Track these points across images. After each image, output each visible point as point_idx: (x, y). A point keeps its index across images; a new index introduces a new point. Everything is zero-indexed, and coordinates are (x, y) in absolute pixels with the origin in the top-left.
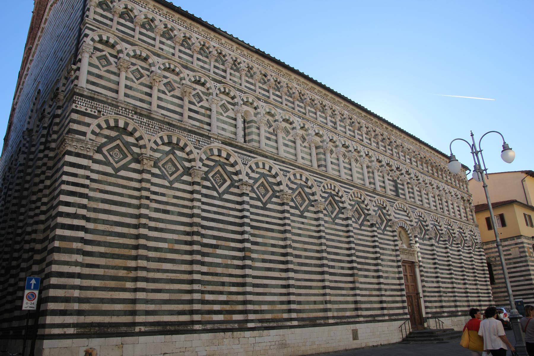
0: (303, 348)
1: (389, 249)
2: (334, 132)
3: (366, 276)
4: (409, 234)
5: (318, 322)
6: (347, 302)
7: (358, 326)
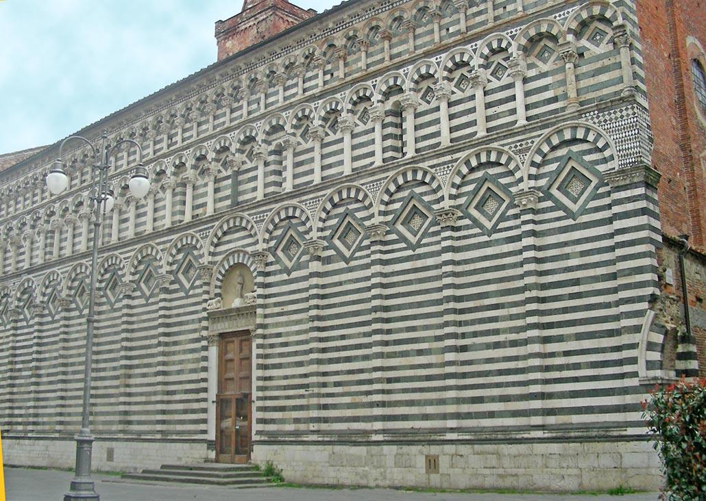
0: (60, 461)
1: (193, 321)
6: (114, 413)
7: (114, 444)
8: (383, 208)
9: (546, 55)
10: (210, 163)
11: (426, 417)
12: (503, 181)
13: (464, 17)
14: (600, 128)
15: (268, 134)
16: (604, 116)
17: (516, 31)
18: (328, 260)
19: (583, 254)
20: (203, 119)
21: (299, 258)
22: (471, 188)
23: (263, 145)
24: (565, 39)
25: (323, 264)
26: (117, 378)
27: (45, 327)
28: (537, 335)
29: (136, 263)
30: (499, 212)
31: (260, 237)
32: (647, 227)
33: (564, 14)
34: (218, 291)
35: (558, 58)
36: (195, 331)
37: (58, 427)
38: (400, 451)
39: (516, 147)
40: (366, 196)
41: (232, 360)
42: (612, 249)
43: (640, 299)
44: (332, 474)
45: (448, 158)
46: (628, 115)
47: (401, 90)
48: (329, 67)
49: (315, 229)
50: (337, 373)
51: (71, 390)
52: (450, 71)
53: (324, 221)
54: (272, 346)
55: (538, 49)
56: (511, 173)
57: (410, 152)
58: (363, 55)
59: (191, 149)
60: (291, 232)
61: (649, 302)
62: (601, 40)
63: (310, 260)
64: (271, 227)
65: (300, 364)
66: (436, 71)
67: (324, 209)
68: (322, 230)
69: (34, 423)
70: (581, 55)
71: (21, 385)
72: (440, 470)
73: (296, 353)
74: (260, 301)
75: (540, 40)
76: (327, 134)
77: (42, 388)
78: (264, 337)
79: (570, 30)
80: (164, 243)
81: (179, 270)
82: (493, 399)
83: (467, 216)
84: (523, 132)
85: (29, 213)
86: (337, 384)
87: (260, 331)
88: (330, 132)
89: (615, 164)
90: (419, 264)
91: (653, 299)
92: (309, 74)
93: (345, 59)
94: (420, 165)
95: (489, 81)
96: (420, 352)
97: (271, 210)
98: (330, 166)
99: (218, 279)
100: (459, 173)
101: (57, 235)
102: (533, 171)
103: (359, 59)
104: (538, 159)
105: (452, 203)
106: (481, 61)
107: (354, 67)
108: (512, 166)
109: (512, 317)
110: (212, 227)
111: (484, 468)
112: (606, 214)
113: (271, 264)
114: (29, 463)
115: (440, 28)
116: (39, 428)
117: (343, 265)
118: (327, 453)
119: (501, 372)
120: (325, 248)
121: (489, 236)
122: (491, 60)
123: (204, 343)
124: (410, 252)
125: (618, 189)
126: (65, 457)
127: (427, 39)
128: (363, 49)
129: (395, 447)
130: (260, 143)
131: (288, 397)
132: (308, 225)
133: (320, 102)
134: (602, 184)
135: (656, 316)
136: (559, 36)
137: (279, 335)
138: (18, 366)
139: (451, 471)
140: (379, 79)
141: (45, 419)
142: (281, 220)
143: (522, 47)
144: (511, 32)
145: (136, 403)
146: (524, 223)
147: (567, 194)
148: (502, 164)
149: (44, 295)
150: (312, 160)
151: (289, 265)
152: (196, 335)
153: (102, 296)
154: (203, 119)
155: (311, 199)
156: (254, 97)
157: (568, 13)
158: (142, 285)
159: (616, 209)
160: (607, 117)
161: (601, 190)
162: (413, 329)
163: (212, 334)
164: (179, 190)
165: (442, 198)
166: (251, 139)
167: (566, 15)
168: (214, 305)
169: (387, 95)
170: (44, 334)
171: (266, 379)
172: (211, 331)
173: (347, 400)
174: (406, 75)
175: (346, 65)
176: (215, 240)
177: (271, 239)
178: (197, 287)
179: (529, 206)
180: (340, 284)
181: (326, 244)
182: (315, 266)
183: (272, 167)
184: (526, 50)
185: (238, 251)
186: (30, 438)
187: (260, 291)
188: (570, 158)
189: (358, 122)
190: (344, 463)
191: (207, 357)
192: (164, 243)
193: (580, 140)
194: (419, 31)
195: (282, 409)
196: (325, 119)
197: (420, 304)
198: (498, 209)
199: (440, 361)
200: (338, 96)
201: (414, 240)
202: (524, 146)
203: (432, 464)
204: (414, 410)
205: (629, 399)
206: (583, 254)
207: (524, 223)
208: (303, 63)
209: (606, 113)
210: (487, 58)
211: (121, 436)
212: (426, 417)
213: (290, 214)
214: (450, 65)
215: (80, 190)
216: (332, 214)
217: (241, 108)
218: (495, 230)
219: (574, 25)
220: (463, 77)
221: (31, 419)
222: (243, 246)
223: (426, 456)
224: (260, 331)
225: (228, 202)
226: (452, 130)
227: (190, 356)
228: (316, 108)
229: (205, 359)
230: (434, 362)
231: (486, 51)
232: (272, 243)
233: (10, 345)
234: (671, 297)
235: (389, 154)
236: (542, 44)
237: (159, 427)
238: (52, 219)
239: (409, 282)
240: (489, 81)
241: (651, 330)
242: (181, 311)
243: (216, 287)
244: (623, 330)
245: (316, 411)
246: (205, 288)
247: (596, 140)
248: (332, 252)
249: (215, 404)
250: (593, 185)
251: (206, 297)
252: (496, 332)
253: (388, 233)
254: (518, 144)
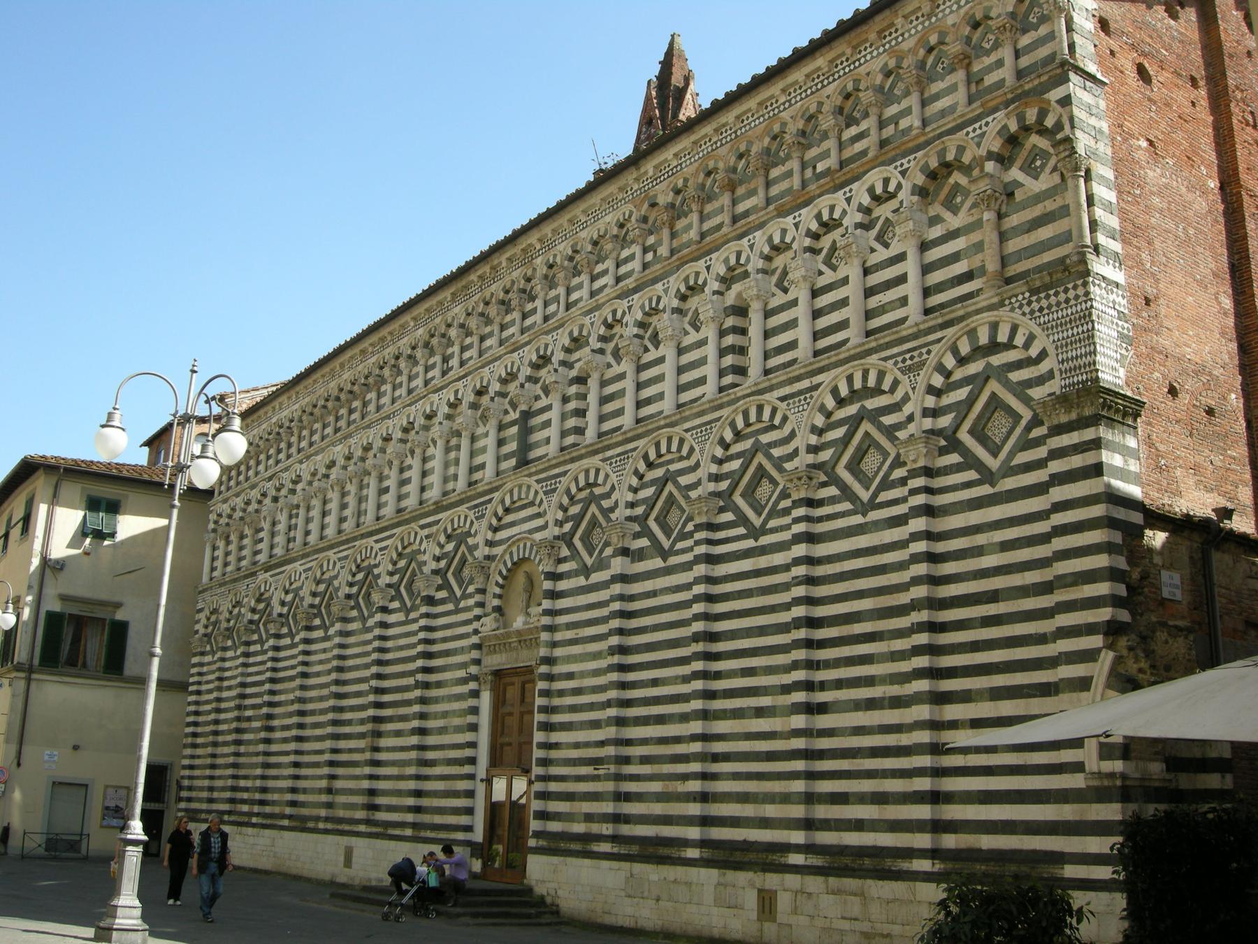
1: (461, 650)
2: (383, 419)
3: (398, 734)
5: (311, 825)
7: (354, 841)
8: (714, 468)
9: (959, 199)
10: (492, 399)
11: (765, 823)
12: (888, 420)
13: (837, 145)
14: (1032, 323)
15: (568, 351)
16: (1038, 301)
17: (909, 162)
18: (639, 555)
19: (1006, 546)
20: (488, 329)
21: (601, 551)
22: (839, 433)
23: (560, 369)
24: (982, 170)
25: (633, 562)
26: (362, 736)
27: (282, 654)
28: (927, 688)
29: (395, 556)
30: (881, 474)
31: (550, 517)
32: (1104, 498)
33: (980, 128)
34: (496, 602)
35: (974, 205)
36: (464, 665)
37: (288, 810)
38: (722, 880)
39: (904, 361)
40: (692, 450)
41: (511, 714)
42: (1044, 539)
43: (1090, 629)
44: (629, 910)
45: (805, 384)
46: (1077, 297)
47: (746, 275)
48: (651, 240)
49: (622, 505)
50: (644, 742)
51: (309, 753)
52: (816, 237)
53: (635, 491)
54: (561, 693)
55: (946, 190)
56: (896, 407)
57: (755, 371)
58: (695, 217)
59: (469, 378)
60: (593, 509)
61: (1106, 634)
62: (1043, 166)
63: (614, 556)
64: (565, 501)
65: (595, 724)
66: (794, 238)
67: (636, 472)
68: (632, 505)
69: (262, 803)
70: (1011, 195)
71: (249, 742)
72: (779, 916)
73: (592, 707)
74: (546, 620)
75: (950, 174)
76: (646, 350)
77: (274, 748)
78: (550, 678)
79: (990, 156)
80: (429, 525)
81: (449, 566)
82: (862, 798)
83: (835, 480)
84: (915, 336)
85: (270, 479)
86: (645, 760)
87: (543, 669)
88: (650, 346)
89: (1054, 386)
90: (763, 562)
91: (1112, 630)
92: (625, 253)
93: (671, 227)
94: (767, 396)
95: (873, 250)
96: (760, 712)
97: (565, 473)
98: (648, 401)
99: (497, 584)
100: (822, 409)
101: (302, 512)
102: (930, 401)
103: (689, 227)
104: (938, 381)
105: (810, 458)
106: (859, 217)
107: (685, 238)
108: (899, 394)
109: (895, 656)
111: (843, 918)
112: (1039, 476)
113: (564, 560)
114: (252, 864)
115: (804, 166)
116: (268, 809)
117: (657, 563)
118: (622, 875)
119: (875, 752)
120: (637, 536)
121: (864, 515)
122: (874, 215)
123: (473, 685)
124: (750, 543)
125: (1057, 430)
126: (293, 857)
127: (784, 185)
128: (694, 207)
129: (714, 873)
130: (556, 366)
131: (579, 779)
132: (614, 497)
133: (636, 296)
134: (1036, 422)
135: (1118, 660)
136: (974, 164)
137: (570, 676)
138: (249, 713)
139: (793, 920)
140: (714, 256)
141: (276, 797)
142: (580, 490)
143: (917, 190)
144: (902, 165)
145: (387, 778)
146: (914, 492)
147: (983, 439)
148: (884, 392)
149: (283, 603)
150: (621, 393)
151: (589, 561)
152: (461, 674)
153: (352, 608)
154: (488, 329)
155: (618, 455)
156: (553, 293)
157: (987, 124)
158: (402, 589)
159: (1056, 466)
160: (1044, 303)
161: (1036, 433)
162: (750, 672)
163: (485, 670)
164: (454, 441)
165: (796, 452)
166: (544, 360)
167: (984, 129)
169: (727, 281)
170: (281, 665)
173: (656, 787)
174: (751, 247)
175: (673, 235)
176: (494, 522)
177: (567, 520)
178: (471, 596)
179: (921, 463)
180: (654, 594)
181: (637, 528)
182: (618, 565)
183: (572, 405)
184: (922, 192)
186: (254, 825)
187: (547, 604)
188: (987, 379)
189: (688, 328)
190: (646, 894)
192: (429, 525)
193: (1004, 345)
194: (775, 173)
195: (569, 797)
196: (642, 325)
197: (762, 631)
198: (879, 468)
199: (787, 729)
200: (659, 287)
201: (757, 521)
202: (916, 360)
203: (767, 902)
204: (748, 810)
205: (1067, 812)
206: (1006, 546)
207: (914, 492)
208: (616, 236)
209: (1042, 295)
210: (867, 211)
211: (362, 828)
212: (765, 823)
213: (591, 481)
214: (814, 226)
215: (333, 444)
216: (646, 479)
217: (534, 311)
218: (873, 505)
219: (996, 146)
220: (834, 248)
221: (257, 796)
222: (531, 532)
223: (760, 891)
224: (543, 669)
225: (513, 462)
226: (816, 336)
227: (456, 706)
228: (630, 308)
229: (475, 711)
230: (779, 729)
231: (866, 200)
232: (568, 527)
233: (239, 680)
234: (1171, 623)
235: (728, 379)
236: (951, 181)
237: (410, 818)
238: (299, 487)
239: (747, 594)
240: (873, 250)
241: (1108, 686)
242: (448, 633)
243: (495, 596)
244: (1061, 685)
245: (611, 804)
246: (478, 598)
247: (1027, 346)
248: (644, 542)
250: (1024, 422)
251: (477, 611)
252: (870, 681)
253: (722, 510)
254: (908, 356)
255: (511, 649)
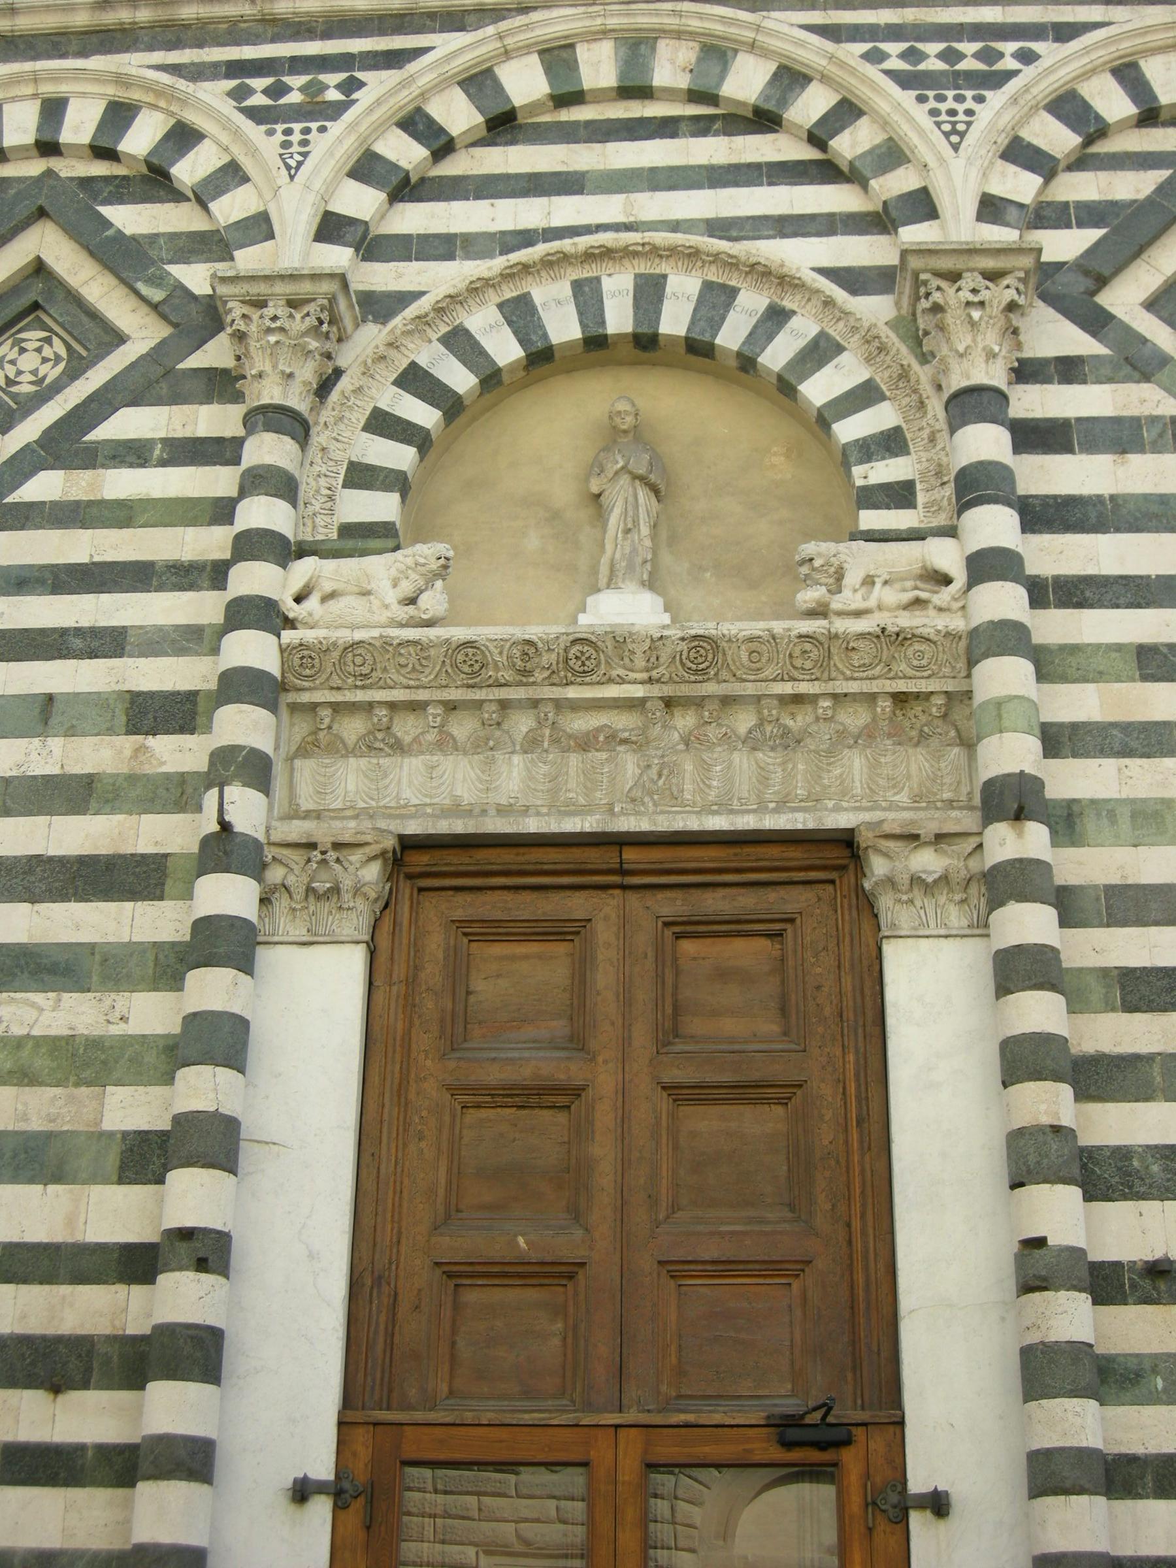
4: (823, 420)
34: (381, 506)
36: (74, 794)
99: (383, 424)
110: (393, 59)
113: (1069, 370)
168: (391, 596)
171: (1107, 1283)
172: (294, 814)
177: (1049, 215)
178: (134, 453)
185: (654, 252)
191: (240, 1026)
222: (719, 227)
243: (361, 476)
249: (321, 1509)
255: (585, 743)
